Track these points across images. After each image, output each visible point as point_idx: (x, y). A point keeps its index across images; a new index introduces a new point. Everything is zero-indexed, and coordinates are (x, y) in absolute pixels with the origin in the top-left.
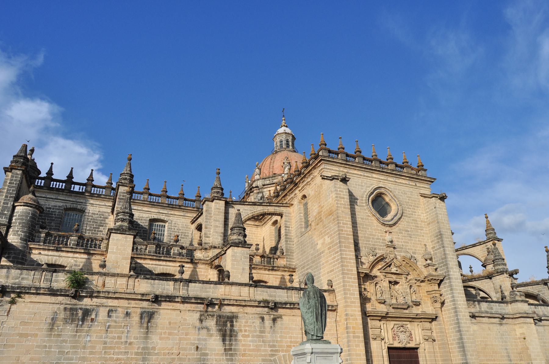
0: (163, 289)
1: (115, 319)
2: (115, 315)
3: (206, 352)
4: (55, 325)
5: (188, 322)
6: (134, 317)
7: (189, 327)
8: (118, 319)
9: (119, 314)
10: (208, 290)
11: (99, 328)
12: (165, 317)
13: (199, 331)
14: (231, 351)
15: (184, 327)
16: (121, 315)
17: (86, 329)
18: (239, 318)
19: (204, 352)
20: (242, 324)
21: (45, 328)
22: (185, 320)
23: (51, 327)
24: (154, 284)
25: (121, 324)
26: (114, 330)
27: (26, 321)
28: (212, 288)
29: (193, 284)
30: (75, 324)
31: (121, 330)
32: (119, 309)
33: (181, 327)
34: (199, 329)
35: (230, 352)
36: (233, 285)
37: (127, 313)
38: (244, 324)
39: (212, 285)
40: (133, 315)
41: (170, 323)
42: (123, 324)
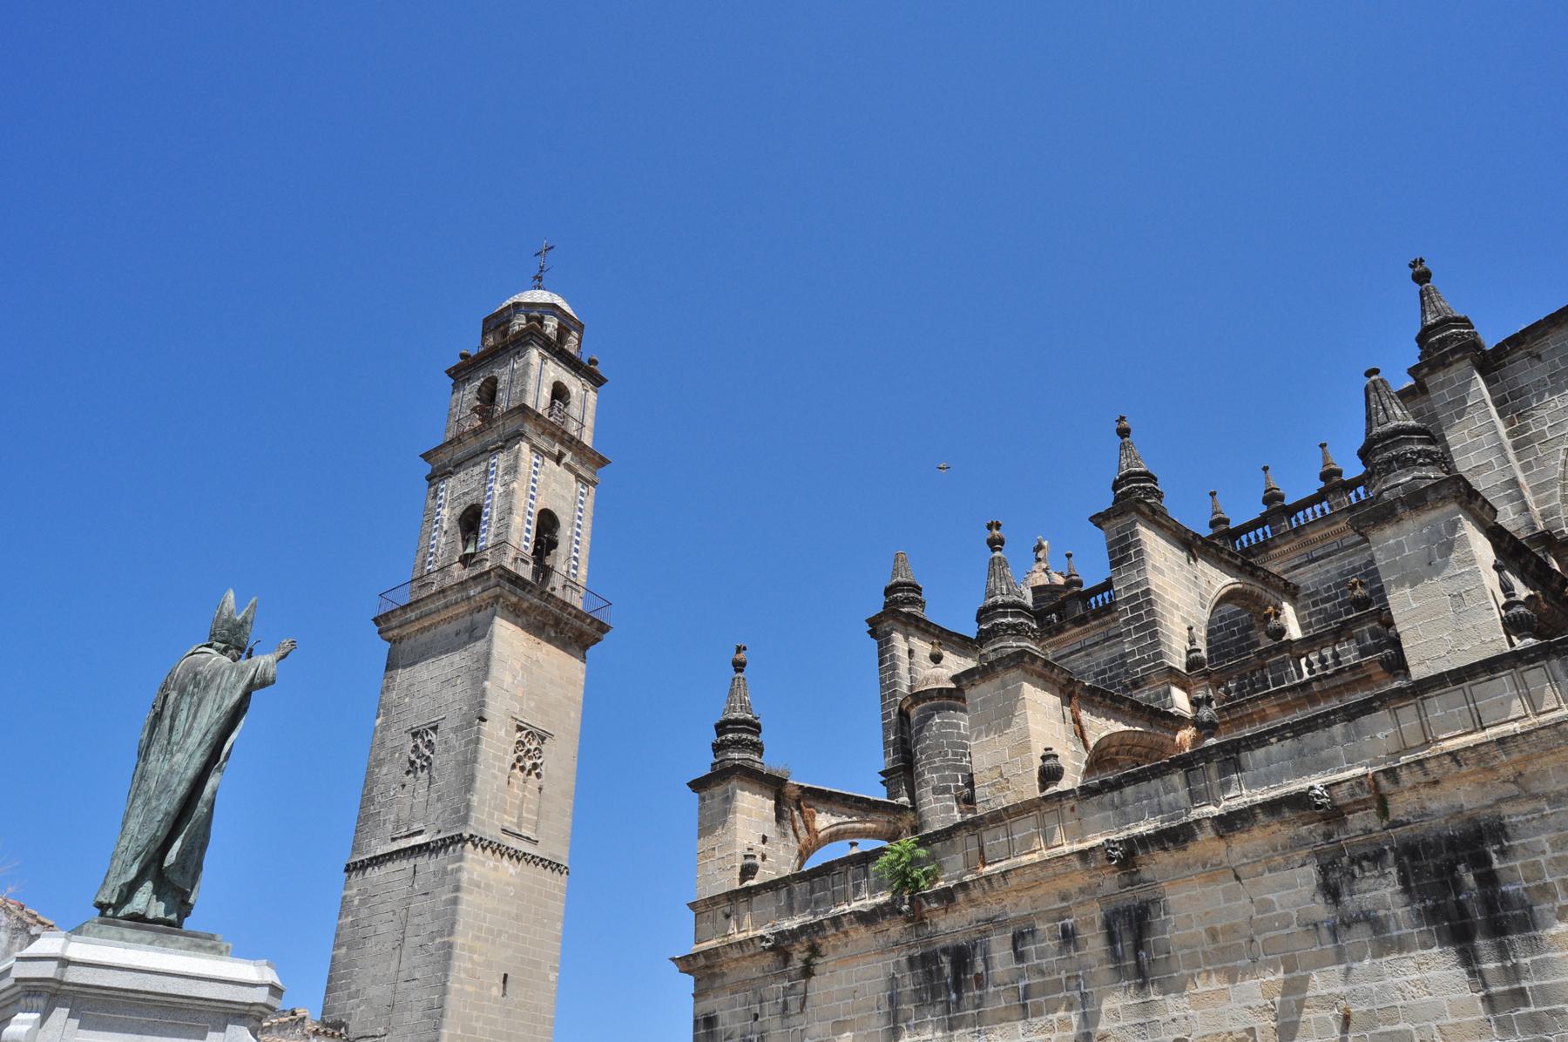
0: (1156, 809)
1: (1036, 962)
2: (1033, 947)
3: (1396, 1028)
4: (901, 1017)
5: (1280, 911)
6: (1089, 940)
7: (1287, 931)
8: (1044, 961)
9: (1043, 941)
10: (1324, 754)
11: (1004, 1004)
12: (1188, 916)
13: (1336, 941)
14: (1527, 1004)
15: (1268, 935)
16: (1051, 943)
17: (970, 1012)
18: (1509, 830)
19: (1388, 1028)
20: (1542, 859)
21: (880, 1030)
22: (1266, 906)
23: (891, 1026)
24: (1124, 803)
25: (1056, 977)
26: (1042, 999)
27: (841, 1019)
28: (1339, 739)
29: (1260, 753)
30: (942, 1002)
31: (1062, 995)
32: (1042, 926)
33: (1259, 940)
34: (1334, 932)
35: (1523, 1011)
36: (1426, 690)
37: (1065, 929)
38: (1549, 854)
39: (1338, 729)
40: (1084, 933)
41: (1213, 934)
42: (1063, 975)
